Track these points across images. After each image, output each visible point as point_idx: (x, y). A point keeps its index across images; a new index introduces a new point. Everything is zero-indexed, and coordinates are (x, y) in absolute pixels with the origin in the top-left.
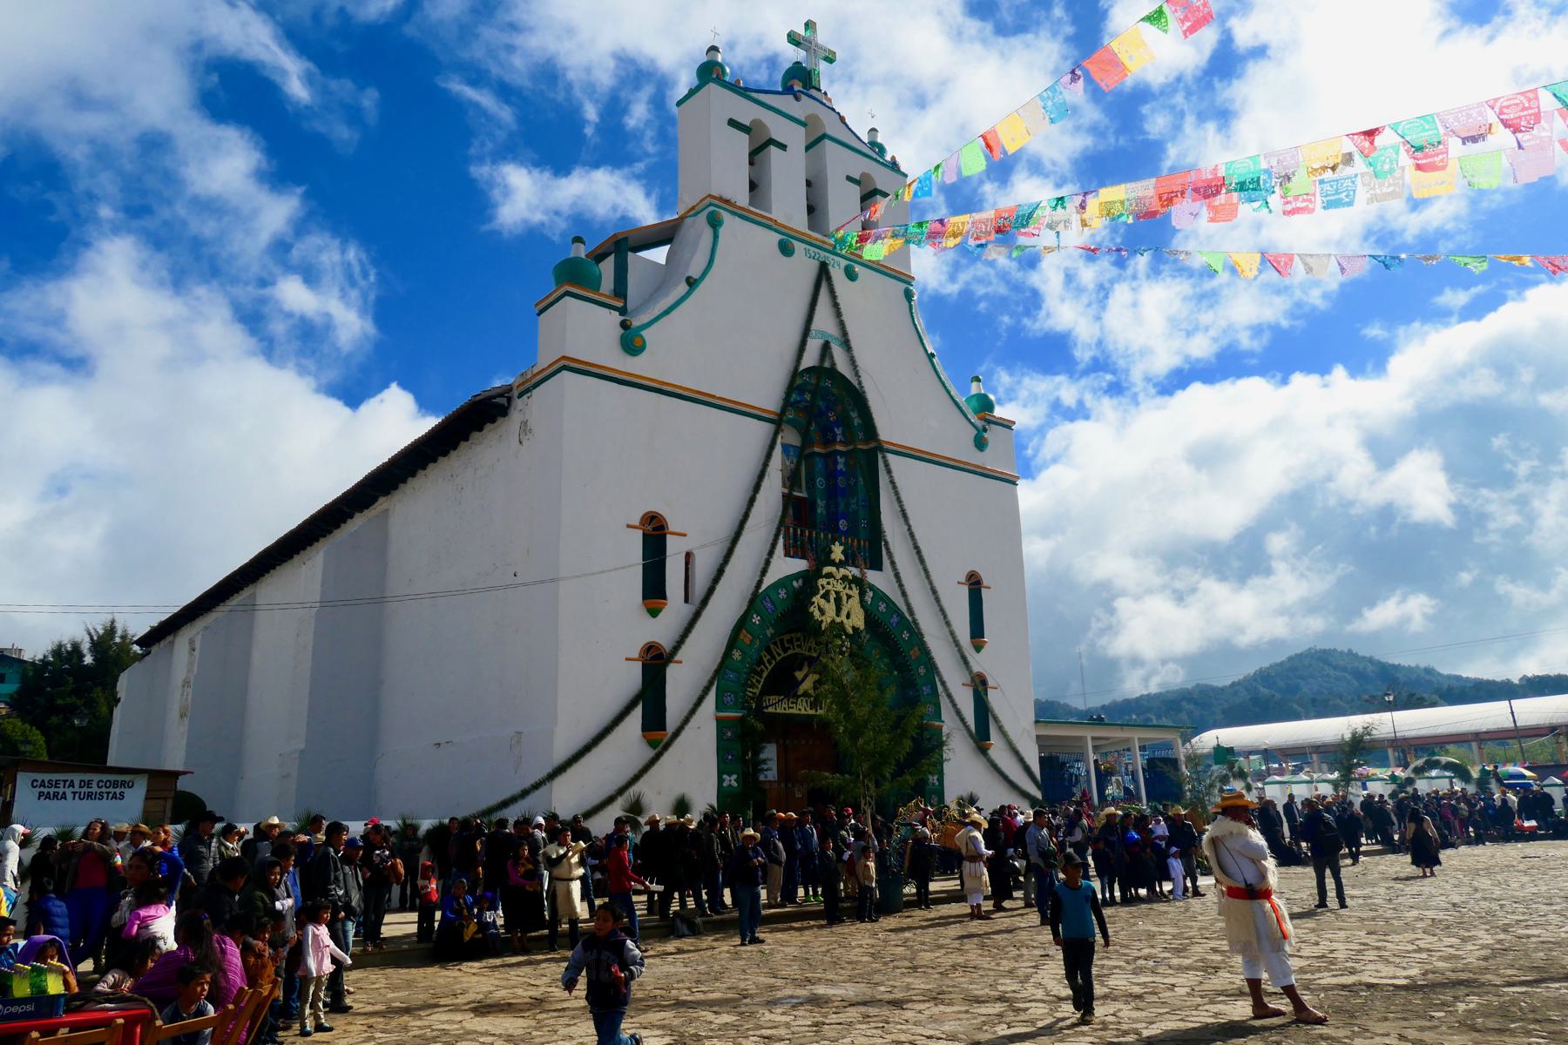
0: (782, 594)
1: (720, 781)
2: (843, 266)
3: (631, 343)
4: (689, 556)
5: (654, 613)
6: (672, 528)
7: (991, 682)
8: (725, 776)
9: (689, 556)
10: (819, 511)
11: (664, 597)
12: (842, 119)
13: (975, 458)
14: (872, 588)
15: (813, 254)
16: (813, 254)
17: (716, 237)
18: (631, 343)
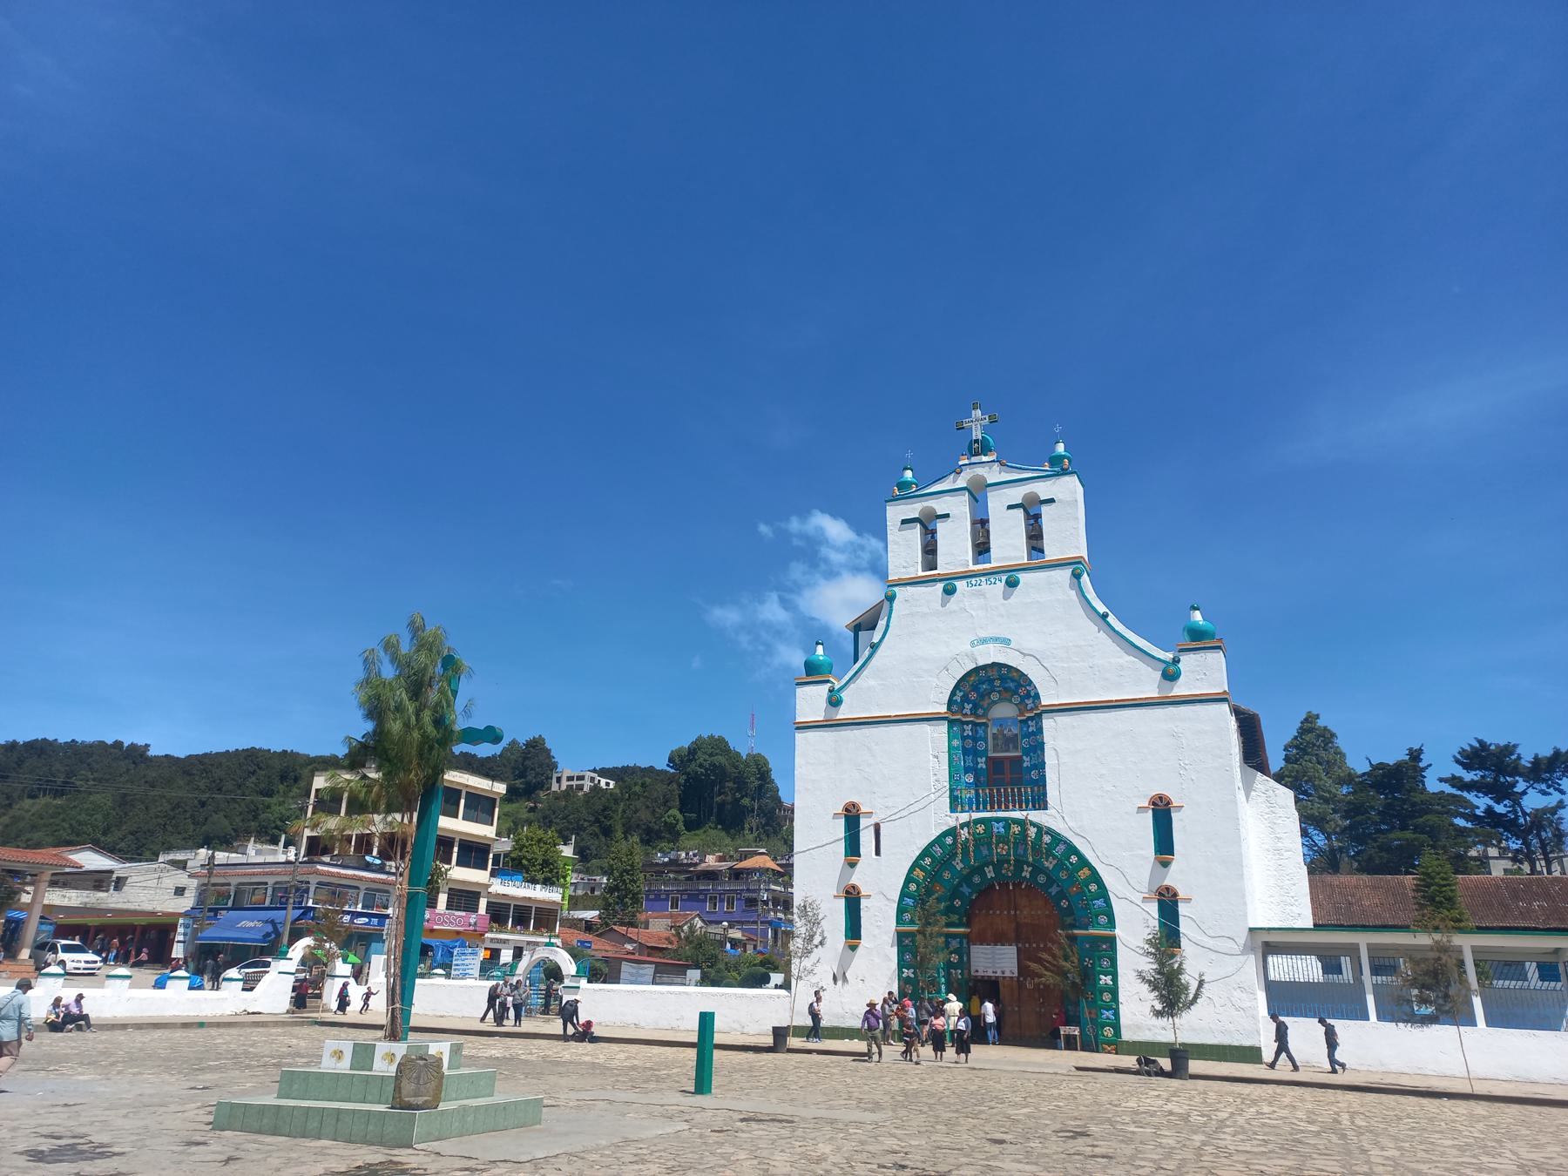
2: (1004, 581)
3: (834, 701)
6: (863, 809)
7: (1181, 895)
11: (860, 856)
14: (1033, 824)
15: (974, 583)
17: (891, 607)
18: (834, 701)
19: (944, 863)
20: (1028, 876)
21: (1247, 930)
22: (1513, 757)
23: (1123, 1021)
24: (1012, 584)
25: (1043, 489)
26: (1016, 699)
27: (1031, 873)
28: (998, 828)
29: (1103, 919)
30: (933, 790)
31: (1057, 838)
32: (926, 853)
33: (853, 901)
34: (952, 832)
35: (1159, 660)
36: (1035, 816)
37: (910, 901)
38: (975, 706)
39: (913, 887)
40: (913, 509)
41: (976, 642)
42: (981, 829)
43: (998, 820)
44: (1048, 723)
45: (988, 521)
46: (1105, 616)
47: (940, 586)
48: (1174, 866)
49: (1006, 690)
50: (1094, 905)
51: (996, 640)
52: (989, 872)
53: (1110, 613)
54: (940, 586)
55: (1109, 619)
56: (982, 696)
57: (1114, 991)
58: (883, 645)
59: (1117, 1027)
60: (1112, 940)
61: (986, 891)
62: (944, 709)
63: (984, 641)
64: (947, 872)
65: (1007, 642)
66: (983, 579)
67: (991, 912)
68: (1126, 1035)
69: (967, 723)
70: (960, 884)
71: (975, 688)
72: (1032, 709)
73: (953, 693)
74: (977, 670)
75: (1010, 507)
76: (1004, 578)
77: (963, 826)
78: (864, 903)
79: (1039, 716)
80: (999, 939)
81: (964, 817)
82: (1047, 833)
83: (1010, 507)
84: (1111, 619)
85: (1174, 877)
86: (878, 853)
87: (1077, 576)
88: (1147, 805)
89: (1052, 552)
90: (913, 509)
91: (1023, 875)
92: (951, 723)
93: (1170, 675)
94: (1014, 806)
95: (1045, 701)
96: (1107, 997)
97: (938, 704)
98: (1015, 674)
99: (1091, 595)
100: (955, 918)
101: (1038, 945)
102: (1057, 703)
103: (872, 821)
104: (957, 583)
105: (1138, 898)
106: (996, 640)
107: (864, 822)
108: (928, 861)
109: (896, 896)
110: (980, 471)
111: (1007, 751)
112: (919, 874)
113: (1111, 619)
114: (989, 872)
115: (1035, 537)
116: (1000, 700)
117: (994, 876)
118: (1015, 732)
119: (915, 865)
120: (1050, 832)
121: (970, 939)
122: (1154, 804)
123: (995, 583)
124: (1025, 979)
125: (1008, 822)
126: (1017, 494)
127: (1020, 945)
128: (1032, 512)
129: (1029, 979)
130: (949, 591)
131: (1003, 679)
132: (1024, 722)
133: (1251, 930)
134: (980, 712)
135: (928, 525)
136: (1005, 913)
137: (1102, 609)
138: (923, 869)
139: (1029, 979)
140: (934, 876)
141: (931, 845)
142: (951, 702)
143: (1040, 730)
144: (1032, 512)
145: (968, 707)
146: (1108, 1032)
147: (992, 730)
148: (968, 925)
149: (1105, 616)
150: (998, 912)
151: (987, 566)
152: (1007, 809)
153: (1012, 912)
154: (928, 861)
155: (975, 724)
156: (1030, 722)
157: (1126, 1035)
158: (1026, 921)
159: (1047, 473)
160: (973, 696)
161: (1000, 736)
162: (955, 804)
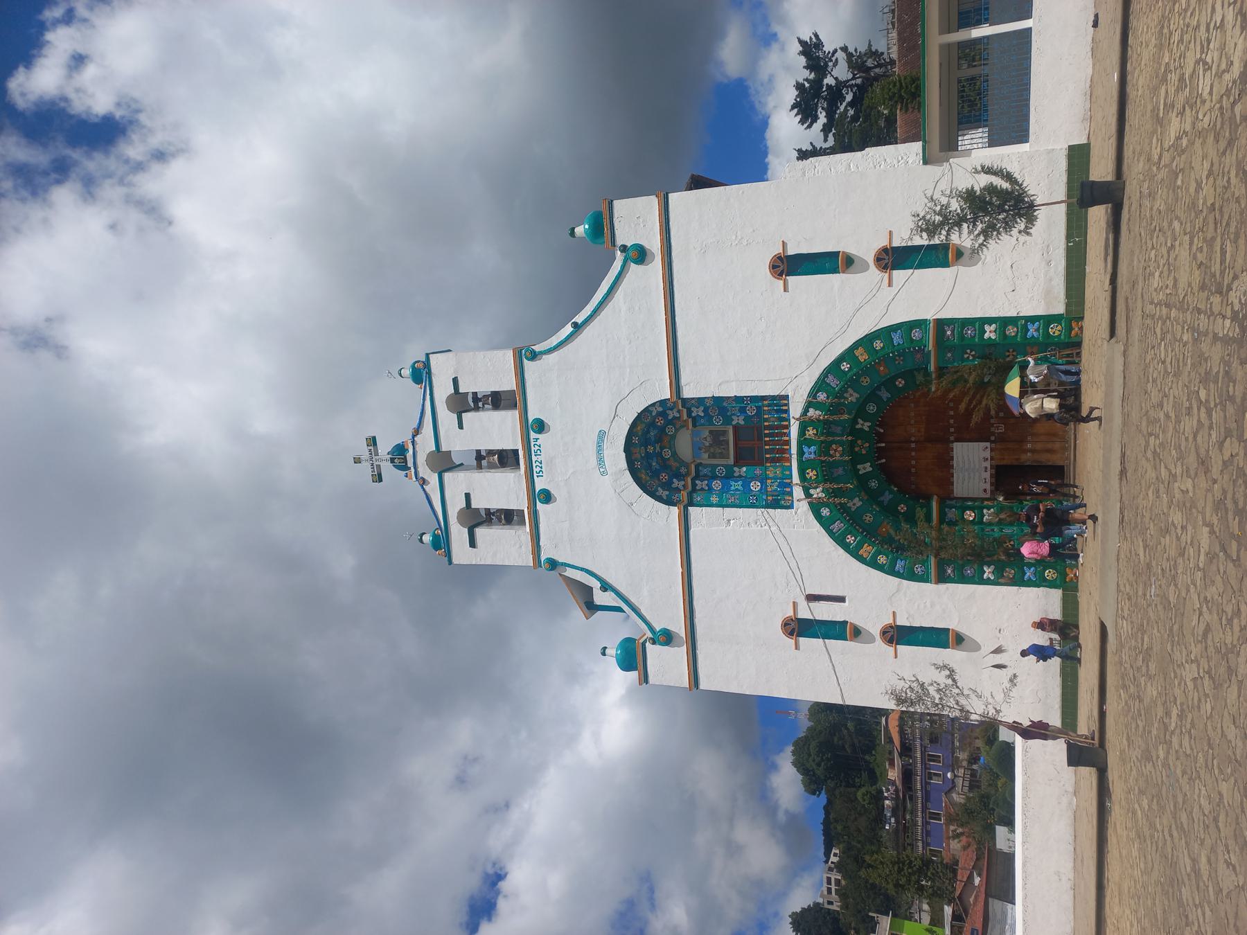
3: (666, 638)
4: (812, 598)
6: (790, 613)
7: (884, 242)
9: (812, 598)
10: (743, 423)
15: (538, 469)
16: (538, 469)
18: (666, 638)
19: (854, 520)
20: (869, 424)
21: (929, 167)
22: (807, 85)
23: (1040, 312)
24: (541, 426)
25: (443, 390)
26: (670, 430)
27: (865, 421)
28: (810, 452)
29: (916, 334)
30: (767, 527)
31: (820, 385)
32: (840, 540)
33: (898, 635)
34: (815, 508)
35: (623, 267)
36: (796, 410)
37: (899, 565)
39: (882, 559)
40: (459, 534)
41: (602, 470)
42: (811, 474)
43: (801, 453)
44: (690, 391)
45: (478, 452)
46: (575, 325)
48: (852, 250)
49: (659, 439)
50: (899, 344)
52: (865, 468)
53: (573, 321)
56: (665, 465)
57: (1004, 322)
58: (604, 576)
59: (1048, 320)
60: (941, 324)
61: (888, 474)
62: (675, 510)
63: (601, 460)
64: (864, 517)
65: (602, 435)
66: (534, 459)
67: (913, 470)
68: (1060, 309)
69: (694, 485)
70: (880, 504)
71: (655, 474)
72: (679, 411)
73: (659, 499)
75: (461, 426)
76: (533, 435)
77: (808, 495)
78: (902, 621)
79: (685, 401)
80: (945, 462)
81: (798, 492)
82: (815, 397)
83: (461, 426)
84: (579, 319)
85: (866, 248)
86: (841, 599)
87: (534, 356)
88: (781, 282)
89: (507, 383)
90: (459, 534)
91: (867, 429)
92: (691, 503)
93: (640, 255)
94: (785, 434)
95: (667, 395)
96: (1011, 331)
98: (639, 428)
99: (554, 341)
100: (920, 513)
101: (952, 417)
102: (668, 381)
103: (802, 603)
105: (887, 293)
107: (804, 614)
108: (850, 539)
109: (893, 581)
110: (421, 459)
111: (727, 442)
112: (867, 550)
113: (579, 319)
114: (865, 468)
115: (497, 400)
117: (869, 464)
118: (707, 433)
119: (855, 554)
120: (813, 393)
121: (947, 499)
122: (781, 275)
123: (540, 446)
124: (993, 434)
125: (803, 441)
126: (447, 418)
127: (952, 438)
128: (463, 403)
129: (993, 429)
130: (547, 497)
131: (646, 442)
132: (695, 420)
133: (926, 162)
134: (683, 470)
135: (476, 519)
136: (913, 454)
137: (568, 329)
138: (860, 546)
139: (993, 429)
140: (869, 533)
141: (831, 533)
142: (669, 502)
143: (700, 401)
144: (463, 403)
145: (676, 483)
146: (1055, 330)
147: (705, 458)
148: (928, 498)
149: (575, 325)
150: (913, 462)
151: (521, 453)
152: (788, 443)
153: (913, 445)
154: (850, 539)
155: (697, 477)
156: (693, 415)
157: (1060, 309)
158: (923, 430)
159: (427, 382)
160: (664, 477)
161: (712, 450)
162: (779, 501)
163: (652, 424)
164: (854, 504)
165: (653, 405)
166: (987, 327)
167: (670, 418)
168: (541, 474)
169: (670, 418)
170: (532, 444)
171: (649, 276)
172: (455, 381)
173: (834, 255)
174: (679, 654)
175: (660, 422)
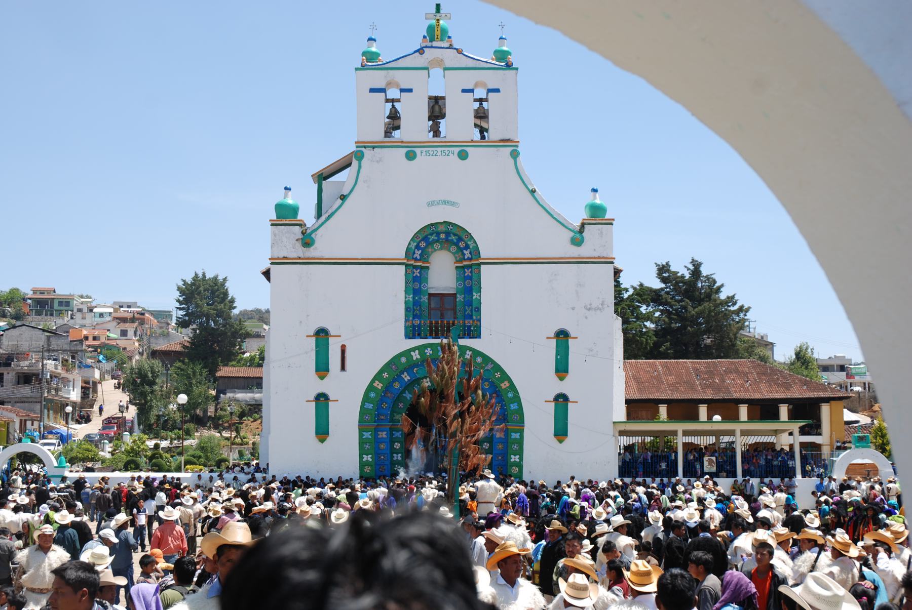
0: (403, 360)
1: (361, 457)
2: (456, 153)
5: (322, 378)
7: (571, 399)
8: (364, 456)
12: (460, 52)
13: (575, 252)
15: (431, 153)
16: (431, 153)
18: (307, 241)
24: (463, 156)
25: (493, 79)
31: (487, 359)
35: (570, 229)
37: (371, 406)
38: (423, 250)
40: (378, 78)
42: (429, 352)
47: (405, 150)
51: (445, 202)
54: (405, 150)
55: (535, 194)
56: (429, 244)
58: (350, 196)
63: (437, 203)
64: (397, 383)
66: (439, 149)
71: (425, 239)
72: (470, 259)
74: (432, 225)
76: (458, 149)
77: (413, 349)
86: (343, 368)
88: (553, 336)
89: (493, 134)
92: (406, 265)
93: (577, 241)
97: (399, 253)
104: (418, 151)
106: (445, 202)
112: (379, 385)
116: (441, 249)
131: (448, 234)
142: (409, 253)
145: (418, 254)
154: (385, 375)
159: (497, 66)
160: (423, 244)
163: (460, 239)
164: (406, 377)
165: (475, 242)
166: (518, 457)
167: (465, 251)
168: (428, 154)
169: (465, 251)
170: (450, 149)
171: (562, 247)
172: (497, 91)
173: (566, 371)
174: (298, 251)
175: (462, 245)
